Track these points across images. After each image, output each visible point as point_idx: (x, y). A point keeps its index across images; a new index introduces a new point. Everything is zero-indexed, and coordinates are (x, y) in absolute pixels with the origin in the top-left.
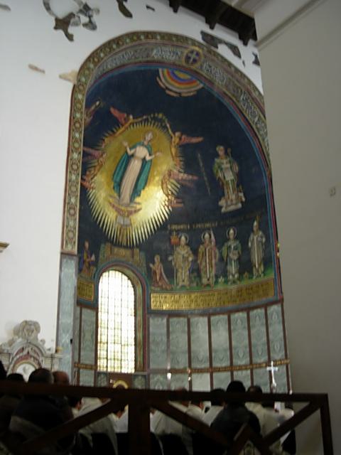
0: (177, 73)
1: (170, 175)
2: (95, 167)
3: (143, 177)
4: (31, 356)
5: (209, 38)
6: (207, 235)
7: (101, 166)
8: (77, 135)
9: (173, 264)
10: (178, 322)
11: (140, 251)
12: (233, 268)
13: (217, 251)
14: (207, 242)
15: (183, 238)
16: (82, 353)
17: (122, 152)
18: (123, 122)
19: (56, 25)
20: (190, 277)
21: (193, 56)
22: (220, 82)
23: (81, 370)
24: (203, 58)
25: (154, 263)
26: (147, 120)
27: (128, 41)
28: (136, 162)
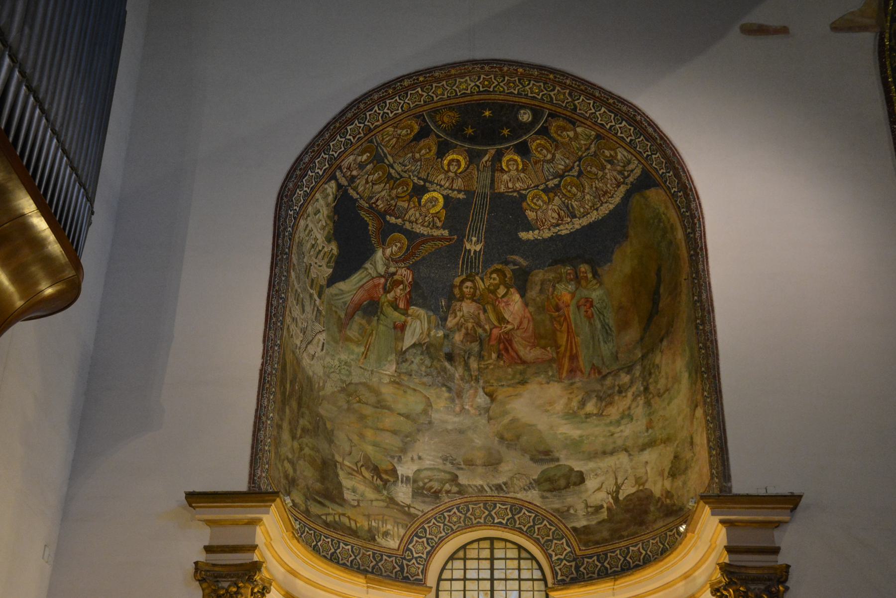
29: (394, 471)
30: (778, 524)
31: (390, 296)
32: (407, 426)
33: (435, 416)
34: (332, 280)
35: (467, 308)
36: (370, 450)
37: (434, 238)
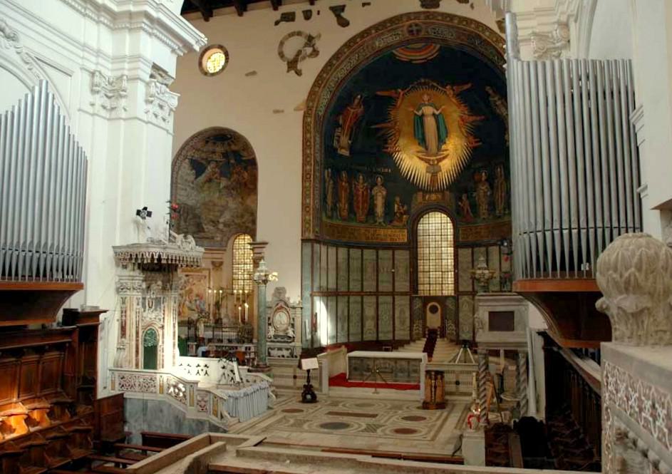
1: (463, 120)
2: (394, 134)
3: (442, 129)
6: (499, 170)
7: (399, 131)
8: (308, 152)
9: (477, 199)
15: (484, 174)
16: (396, 284)
18: (397, 95)
19: (289, 68)
21: (414, 28)
22: (451, 37)
23: (396, 297)
24: (424, 26)
27: (346, 50)
28: (429, 119)
29: (218, 222)
30: (264, 247)
31: (215, 176)
32: (221, 209)
33: (229, 205)
34: (196, 178)
35: (235, 176)
36: (211, 217)
37: (221, 162)
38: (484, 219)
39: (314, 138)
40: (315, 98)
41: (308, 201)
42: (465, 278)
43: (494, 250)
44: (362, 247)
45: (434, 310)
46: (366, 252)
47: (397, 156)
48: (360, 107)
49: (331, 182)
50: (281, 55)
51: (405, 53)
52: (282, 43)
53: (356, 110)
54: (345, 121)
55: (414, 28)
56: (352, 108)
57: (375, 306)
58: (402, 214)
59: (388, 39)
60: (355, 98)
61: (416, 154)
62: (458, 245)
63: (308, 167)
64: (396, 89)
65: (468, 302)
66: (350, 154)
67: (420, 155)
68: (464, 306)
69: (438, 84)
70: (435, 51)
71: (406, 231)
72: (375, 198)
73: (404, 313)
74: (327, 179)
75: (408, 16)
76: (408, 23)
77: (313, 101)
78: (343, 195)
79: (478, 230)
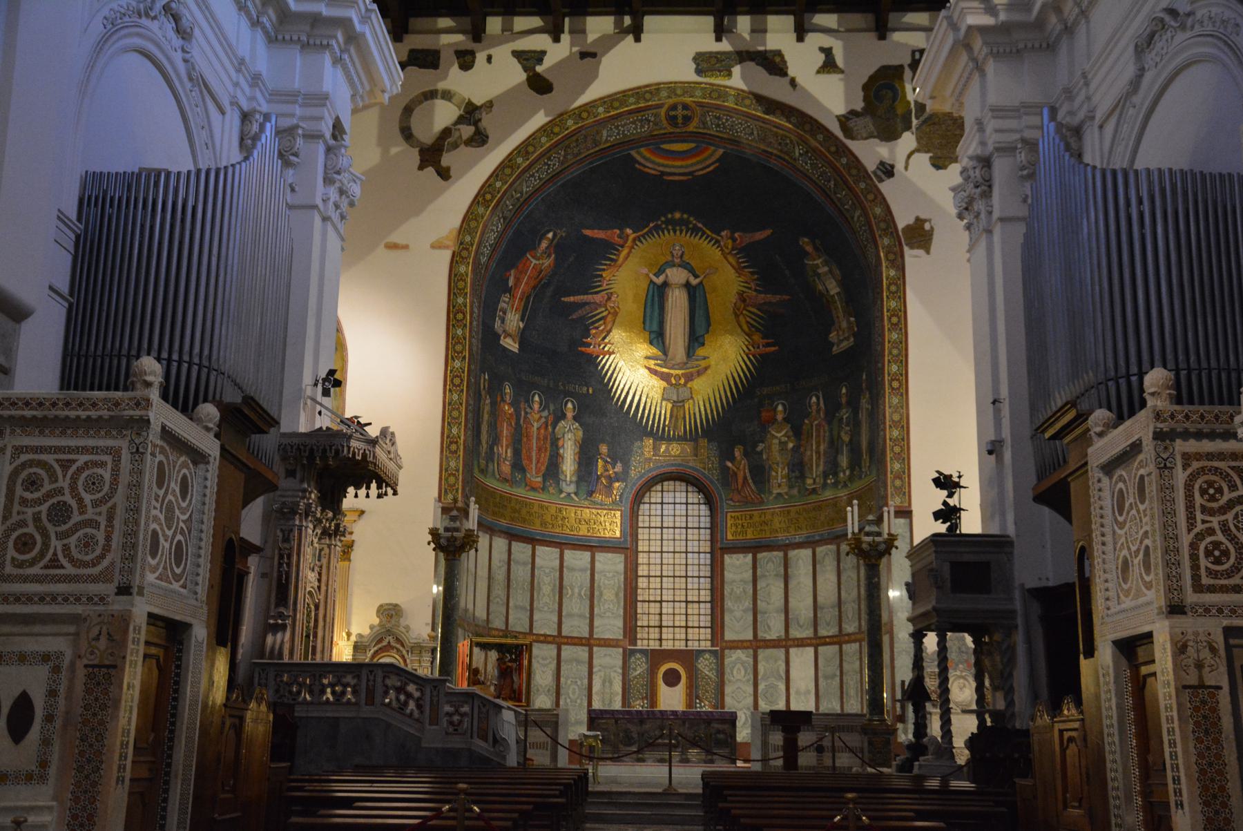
0: (664, 146)
1: (744, 301)
3: (699, 313)
4: (393, 648)
5: (713, 61)
6: (814, 399)
7: (616, 314)
8: (459, 332)
9: (764, 457)
10: (770, 560)
11: (709, 441)
12: (844, 461)
13: (826, 428)
14: (814, 413)
15: (780, 408)
17: (644, 285)
18: (621, 241)
19: (421, 161)
20: (790, 480)
21: (680, 112)
23: (595, 649)
25: (732, 459)
26: (657, 228)
27: (544, 140)
38: (779, 494)
39: (471, 307)
40: (477, 227)
41: (455, 431)
42: (738, 614)
43: (802, 557)
44: (533, 541)
45: (672, 679)
46: (541, 550)
47: (609, 362)
48: (549, 256)
49: (488, 401)
50: (407, 134)
51: (653, 158)
52: (408, 111)
53: (540, 261)
54: (518, 280)
55: (680, 112)
56: (533, 257)
57: (553, 665)
58: (611, 480)
59: (632, 129)
60: (544, 235)
61: (646, 363)
62: (719, 550)
63: (457, 364)
64: (621, 229)
65: (743, 663)
66: (519, 350)
67: (652, 363)
68: (735, 672)
69: (705, 225)
70: (710, 161)
71: (618, 514)
72: (560, 443)
73: (611, 683)
74: (483, 393)
75: (672, 87)
76: (671, 101)
77: (471, 232)
78: (505, 431)
79: (768, 517)
